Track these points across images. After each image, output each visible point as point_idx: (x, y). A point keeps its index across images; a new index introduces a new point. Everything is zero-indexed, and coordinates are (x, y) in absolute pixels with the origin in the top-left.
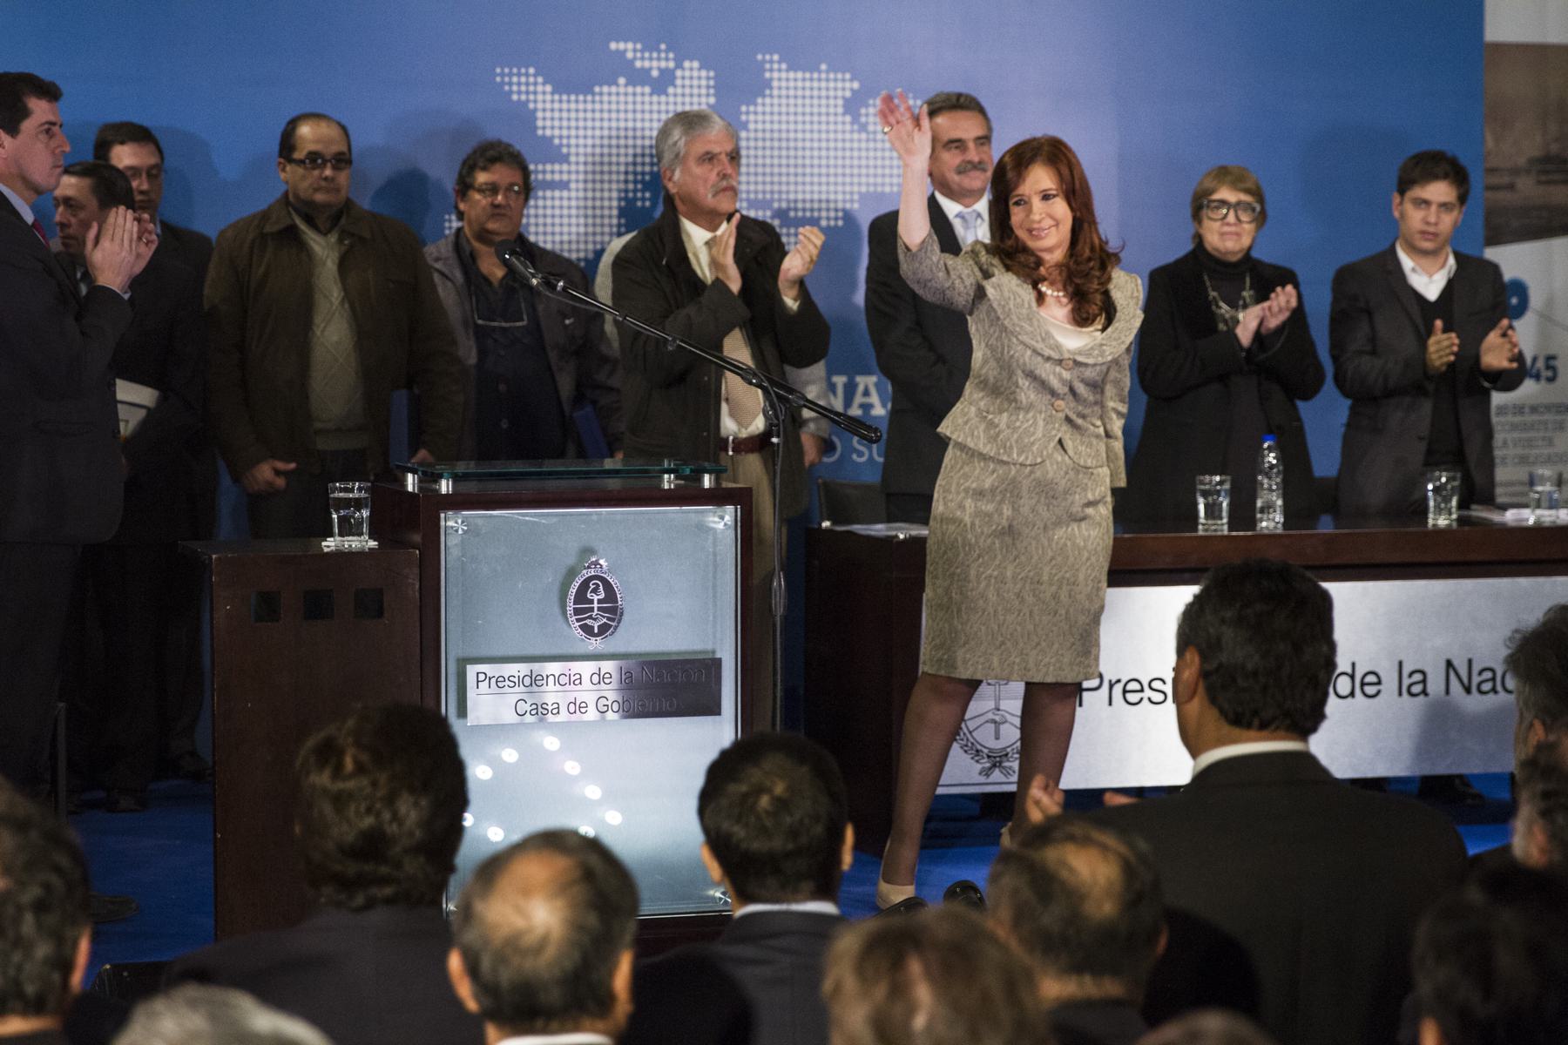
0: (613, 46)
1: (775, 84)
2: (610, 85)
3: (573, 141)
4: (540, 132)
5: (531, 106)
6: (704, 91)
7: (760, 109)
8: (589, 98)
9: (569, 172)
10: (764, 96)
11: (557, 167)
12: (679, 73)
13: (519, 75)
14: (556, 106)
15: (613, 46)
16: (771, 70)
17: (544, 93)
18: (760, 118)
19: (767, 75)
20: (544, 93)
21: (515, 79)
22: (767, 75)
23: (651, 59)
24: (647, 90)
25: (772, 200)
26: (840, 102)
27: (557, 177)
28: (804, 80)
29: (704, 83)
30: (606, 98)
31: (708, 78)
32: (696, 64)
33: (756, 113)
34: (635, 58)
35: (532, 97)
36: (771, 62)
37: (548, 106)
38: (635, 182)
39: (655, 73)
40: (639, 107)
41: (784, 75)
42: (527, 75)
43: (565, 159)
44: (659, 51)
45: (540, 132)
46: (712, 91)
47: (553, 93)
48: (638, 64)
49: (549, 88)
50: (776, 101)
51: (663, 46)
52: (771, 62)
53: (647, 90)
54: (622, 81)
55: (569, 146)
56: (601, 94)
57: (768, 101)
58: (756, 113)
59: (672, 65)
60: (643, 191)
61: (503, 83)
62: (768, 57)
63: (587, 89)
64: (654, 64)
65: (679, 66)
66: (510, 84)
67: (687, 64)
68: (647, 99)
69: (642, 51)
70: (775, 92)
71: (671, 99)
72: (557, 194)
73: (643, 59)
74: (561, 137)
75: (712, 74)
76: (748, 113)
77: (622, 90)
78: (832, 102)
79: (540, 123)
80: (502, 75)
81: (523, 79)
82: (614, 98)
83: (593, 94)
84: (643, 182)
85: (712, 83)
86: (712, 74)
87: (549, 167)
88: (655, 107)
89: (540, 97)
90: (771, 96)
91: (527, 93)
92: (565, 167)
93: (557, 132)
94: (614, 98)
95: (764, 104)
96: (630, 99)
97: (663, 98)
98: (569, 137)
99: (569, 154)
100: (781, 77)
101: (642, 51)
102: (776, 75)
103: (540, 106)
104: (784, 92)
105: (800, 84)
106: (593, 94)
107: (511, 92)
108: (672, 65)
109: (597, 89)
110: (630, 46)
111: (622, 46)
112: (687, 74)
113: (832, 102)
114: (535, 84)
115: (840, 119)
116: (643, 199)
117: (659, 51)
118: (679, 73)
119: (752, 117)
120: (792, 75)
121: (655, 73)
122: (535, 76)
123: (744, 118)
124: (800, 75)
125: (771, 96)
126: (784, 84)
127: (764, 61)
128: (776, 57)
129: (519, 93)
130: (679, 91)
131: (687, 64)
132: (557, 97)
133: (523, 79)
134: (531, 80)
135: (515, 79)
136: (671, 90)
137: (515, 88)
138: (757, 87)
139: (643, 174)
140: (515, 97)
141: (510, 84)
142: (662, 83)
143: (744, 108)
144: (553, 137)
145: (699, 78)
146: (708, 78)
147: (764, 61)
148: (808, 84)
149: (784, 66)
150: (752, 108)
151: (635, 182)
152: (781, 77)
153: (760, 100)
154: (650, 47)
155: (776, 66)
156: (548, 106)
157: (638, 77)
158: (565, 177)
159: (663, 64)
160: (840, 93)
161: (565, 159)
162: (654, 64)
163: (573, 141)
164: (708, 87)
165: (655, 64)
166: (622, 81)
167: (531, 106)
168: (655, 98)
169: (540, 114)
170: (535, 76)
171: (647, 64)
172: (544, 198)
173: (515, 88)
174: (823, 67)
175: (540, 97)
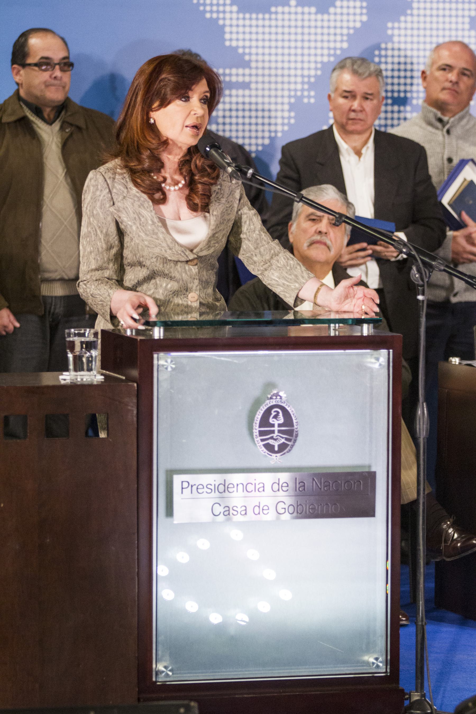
4: (227, 43)
5: (221, 22)
6: (358, 11)
7: (403, 25)
8: (267, 16)
9: (250, 75)
10: (406, 15)
11: (241, 71)
17: (231, 12)
18: (403, 32)
24: (313, 10)
26: (467, 20)
27: (240, 79)
33: (399, 28)
37: (234, 22)
38: (303, 83)
43: (247, 65)
45: (227, 43)
46: (364, 11)
47: (238, 12)
50: (415, 19)
55: (250, 54)
56: (276, 13)
57: (409, 18)
58: (399, 28)
60: (309, 90)
63: (265, 9)
68: (313, 17)
70: (415, 12)
71: (332, 17)
72: (241, 92)
76: (393, 28)
77: (293, 10)
78: (460, 20)
79: (227, 36)
84: (309, 83)
87: (234, 71)
88: (319, 24)
89: (228, 16)
90: (412, 15)
92: (247, 71)
93: (241, 44)
95: (406, 22)
96: (299, 17)
97: (326, 17)
99: (250, 61)
103: (228, 22)
106: (270, 13)
107: (205, 11)
109: (273, 9)
113: (460, 20)
116: (309, 97)
123: (390, 32)
125: (412, 15)
129: (211, 12)
132: (241, 16)
136: (332, 10)
139: (309, 76)
143: (390, 25)
144: (237, 47)
150: (396, 25)
151: (303, 83)
153: (402, 18)
156: (234, 22)
158: (247, 79)
160: (466, 13)
161: (247, 65)
167: (221, 22)
168: (319, 17)
169: (227, 29)
172: (230, 96)
175: (228, 16)
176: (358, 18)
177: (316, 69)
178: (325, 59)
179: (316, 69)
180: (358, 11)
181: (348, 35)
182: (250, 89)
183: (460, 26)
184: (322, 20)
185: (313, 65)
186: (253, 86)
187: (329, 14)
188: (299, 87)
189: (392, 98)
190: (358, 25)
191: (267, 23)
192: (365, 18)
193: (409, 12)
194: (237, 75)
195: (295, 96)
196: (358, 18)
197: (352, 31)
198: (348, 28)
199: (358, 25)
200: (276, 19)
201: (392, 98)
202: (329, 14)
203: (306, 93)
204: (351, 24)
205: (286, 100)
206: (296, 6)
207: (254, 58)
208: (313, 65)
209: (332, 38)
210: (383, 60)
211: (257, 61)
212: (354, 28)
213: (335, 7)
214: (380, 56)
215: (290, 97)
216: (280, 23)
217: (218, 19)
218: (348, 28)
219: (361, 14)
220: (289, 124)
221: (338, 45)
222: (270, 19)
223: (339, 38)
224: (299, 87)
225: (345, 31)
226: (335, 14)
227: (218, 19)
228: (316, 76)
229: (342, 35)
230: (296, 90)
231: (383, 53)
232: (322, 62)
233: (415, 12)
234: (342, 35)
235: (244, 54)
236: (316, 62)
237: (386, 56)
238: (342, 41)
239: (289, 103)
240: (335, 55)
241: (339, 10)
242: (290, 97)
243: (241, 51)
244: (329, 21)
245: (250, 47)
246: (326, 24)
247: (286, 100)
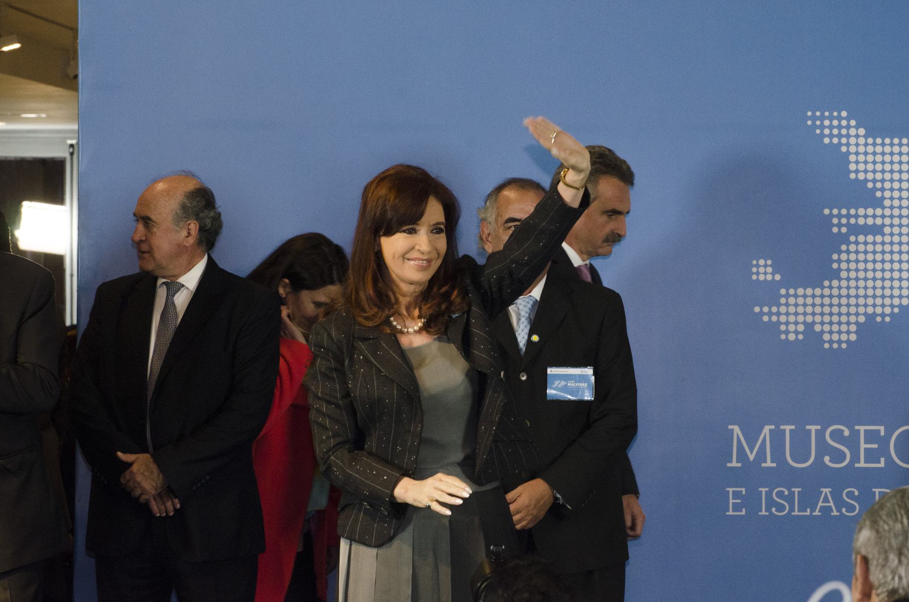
3: (887, 185)
9: (883, 216)
11: (870, 211)
13: (831, 118)
14: (870, 149)
17: (857, 136)
20: (857, 136)
21: (827, 123)
27: (870, 221)
35: (844, 140)
37: (861, 149)
42: (840, 118)
43: (879, 203)
47: (866, 136)
49: (862, 131)
55: (883, 190)
61: (814, 126)
66: (822, 127)
72: (870, 238)
74: (874, 181)
79: (852, 167)
80: (813, 118)
81: (835, 123)
87: (861, 211)
91: (840, 136)
92: (879, 212)
93: (870, 176)
98: (883, 181)
99: (883, 198)
103: (853, 149)
107: (823, 135)
114: (848, 127)
122: (848, 119)
129: (831, 136)
132: (870, 140)
133: (835, 123)
134: (844, 123)
135: (827, 123)
137: (827, 131)
140: (827, 141)
141: (822, 127)
144: (866, 180)
156: (861, 149)
158: (879, 221)
161: (879, 203)
163: (887, 185)
169: (852, 158)
170: (848, 119)
172: (857, 243)
173: (827, 131)
175: (853, 141)
182: (883, 235)
186: (887, 230)
194: (866, 216)
207: (887, 194)
211: (892, 199)
217: (840, 144)
227: (840, 144)
235: (875, 189)
243: (870, 185)
245: (883, 181)
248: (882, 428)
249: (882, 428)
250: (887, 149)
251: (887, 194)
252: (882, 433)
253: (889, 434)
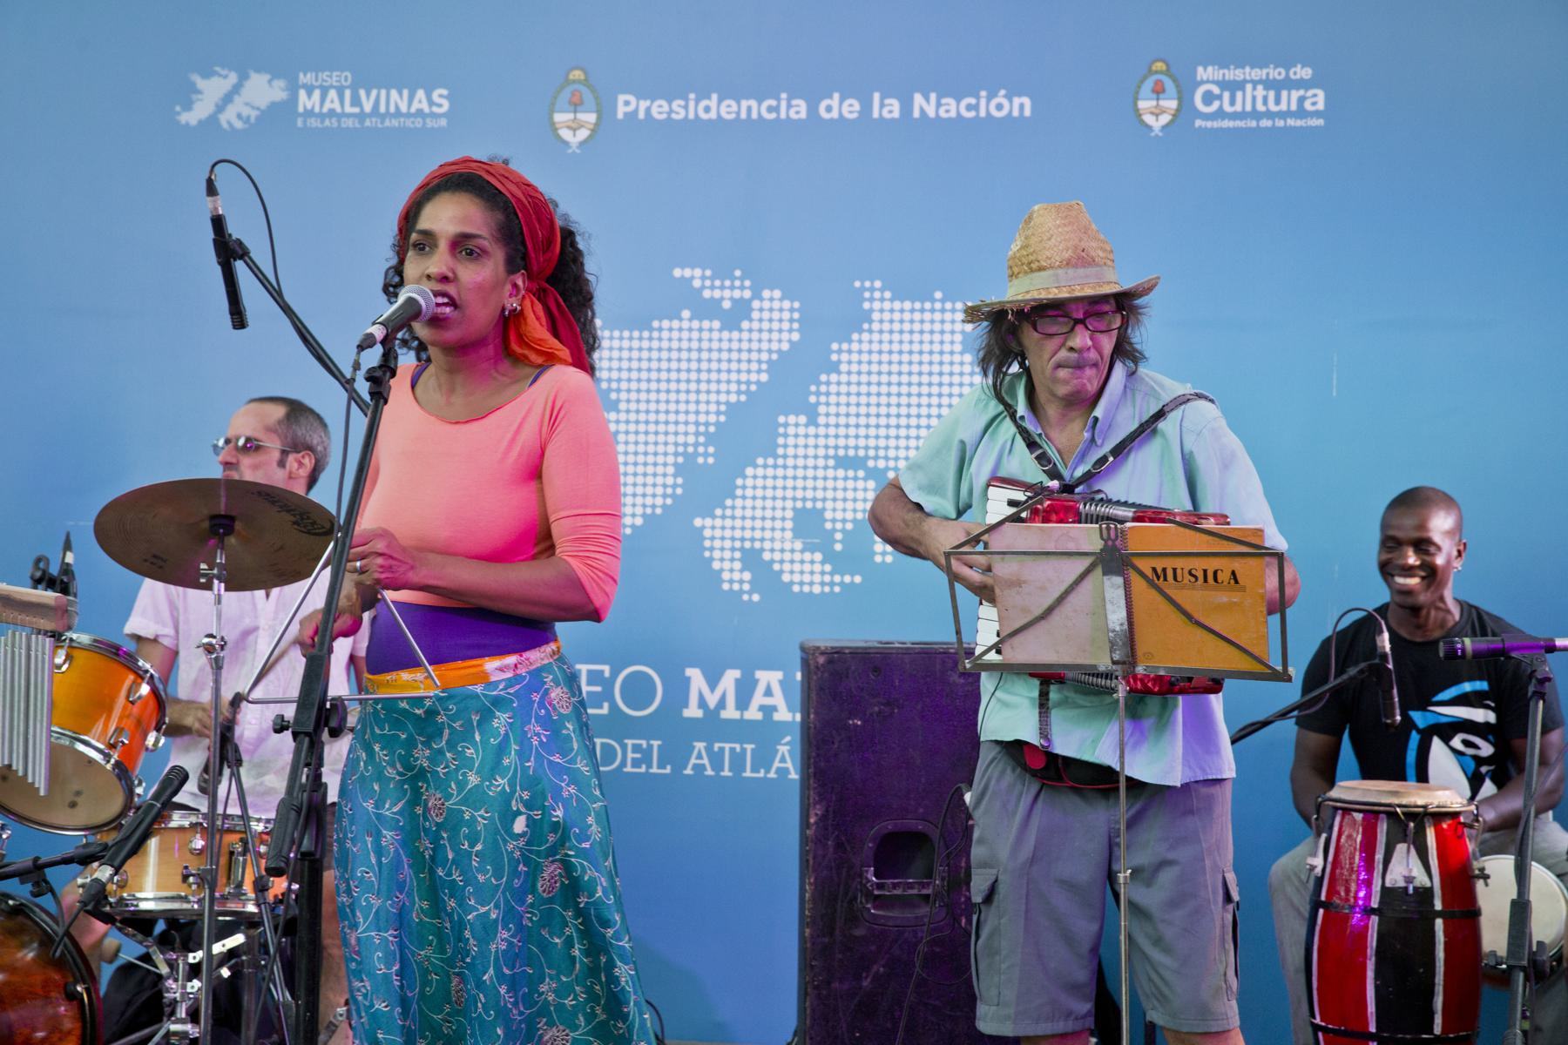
0: (677, 273)
1: (876, 316)
2: (671, 319)
3: (624, 385)
6: (786, 326)
7: (855, 347)
8: (646, 334)
10: (861, 331)
12: (756, 304)
15: (677, 273)
16: (872, 300)
18: (855, 357)
19: (866, 305)
22: (866, 305)
23: (722, 288)
24: (716, 324)
25: (867, 457)
28: (912, 311)
29: (786, 315)
30: (665, 334)
31: (792, 310)
32: (777, 294)
34: (703, 287)
36: (872, 290)
38: (697, 434)
39: (727, 305)
40: (705, 345)
41: (887, 305)
44: (733, 278)
46: (796, 326)
48: (707, 294)
50: (876, 337)
51: (738, 273)
52: (872, 290)
53: (716, 324)
54: (686, 314)
55: (618, 391)
56: (660, 329)
57: (865, 336)
58: (850, 352)
59: (747, 294)
60: (706, 445)
62: (867, 284)
64: (727, 295)
65: (757, 295)
67: (766, 294)
68: (715, 335)
69: (712, 278)
70: (876, 326)
71: (745, 335)
73: (712, 288)
75: (796, 305)
76: (840, 351)
78: (947, 337)
82: (675, 335)
83: (651, 329)
84: (707, 434)
85: (796, 315)
86: (796, 305)
88: (725, 345)
94: (675, 335)
95: (862, 341)
96: (695, 335)
97: (735, 335)
100: (882, 306)
101: (712, 278)
102: (877, 305)
104: (886, 327)
105: (907, 316)
106: (651, 329)
108: (747, 294)
109: (656, 324)
110: (698, 272)
111: (687, 273)
112: (766, 305)
113: (947, 337)
115: (957, 358)
117: (733, 278)
118: (756, 304)
119: (845, 357)
120: (897, 305)
121: (727, 305)
124: (907, 305)
125: (870, 331)
126: (887, 316)
127: (863, 289)
128: (878, 284)
130: (755, 325)
131: (766, 294)
136: (745, 325)
138: (858, 320)
139: (707, 424)
142: (736, 316)
143: (835, 346)
145: (781, 310)
146: (792, 310)
147: (863, 289)
148: (917, 316)
149: (888, 295)
150: (845, 346)
151: (697, 434)
152: (882, 306)
153: (855, 336)
154: (722, 273)
155: (877, 295)
157: (705, 310)
159: (737, 294)
162: (727, 295)
163: (624, 385)
164: (791, 321)
165: (727, 293)
166: (686, 314)
168: (726, 335)
171: (717, 294)
174: (938, 295)
176: (785, 336)
177: (718, 413)
178: (733, 398)
179: (718, 413)
180: (786, 326)
181: (769, 362)
183: (947, 347)
184: (730, 340)
185: (713, 408)
187: (741, 330)
188: (691, 439)
189: (836, 457)
190: (785, 347)
191: (645, 344)
192: (796, 337)
193: (866, 326)
195: (685, 454)
196: (785, 336)
197: (775, 356)
198: (770, 351)
199: (785, 347)
200: (660, 339)
201: (836, 457)
202: (741, 330)
203: (701, 449)
204: (775, 346)
205: (671, 459)
206: (690, 320)
207: (623, 396)
208: (713, 408)
209: (744, 366)
210: (823, 399)
212: (779, 351)
213: (751, 320)
214: (818, 394)
215: (676, 454)
216: (665, 344)
218: (770, 351)
219: (791, 331)
220: (673, 496)
221: (754, 377)
222: (651, 339)
223: (754, 366)
224: (691, 439)
225: (765, 356)
226: (750, 330)
228: (717, 424)
229: (759, 362)
230: (686, 445)
231: (823, 388)
232: (727, 403)
233: (876, 326)
234: (759, 362)
236: (718, 403)
237: (828, 394)
238: (759, 371)
239: (675, 464)
240: (747, 392)
241: (755, 325)
242: (676, 454)
244: (740, 340)
245: (619, 380)
246: (735, 345)
247: (671, 459)
248: (606, 669)
249: (606, 669)
250: (626, 344)
251: (623, 396)
252: (607, 674)
253: (615, 674)
